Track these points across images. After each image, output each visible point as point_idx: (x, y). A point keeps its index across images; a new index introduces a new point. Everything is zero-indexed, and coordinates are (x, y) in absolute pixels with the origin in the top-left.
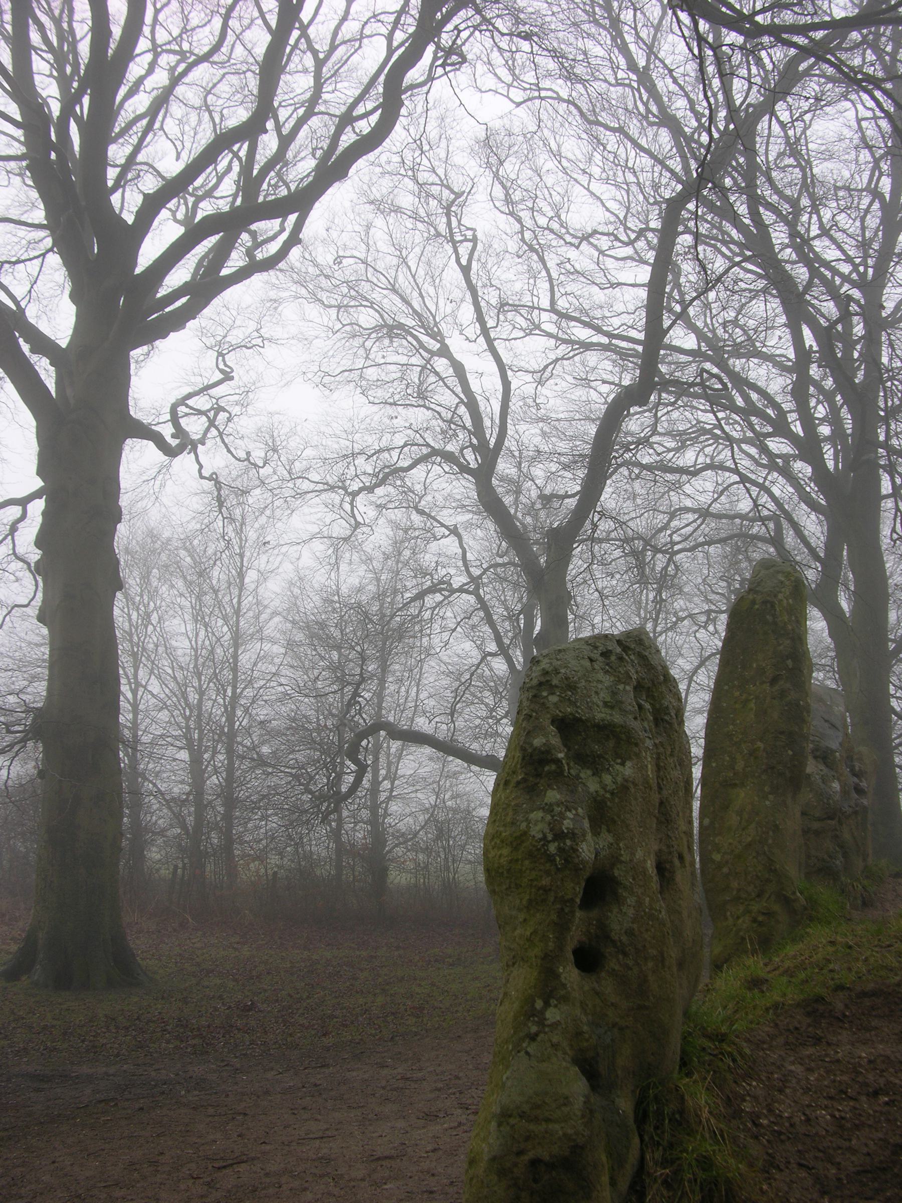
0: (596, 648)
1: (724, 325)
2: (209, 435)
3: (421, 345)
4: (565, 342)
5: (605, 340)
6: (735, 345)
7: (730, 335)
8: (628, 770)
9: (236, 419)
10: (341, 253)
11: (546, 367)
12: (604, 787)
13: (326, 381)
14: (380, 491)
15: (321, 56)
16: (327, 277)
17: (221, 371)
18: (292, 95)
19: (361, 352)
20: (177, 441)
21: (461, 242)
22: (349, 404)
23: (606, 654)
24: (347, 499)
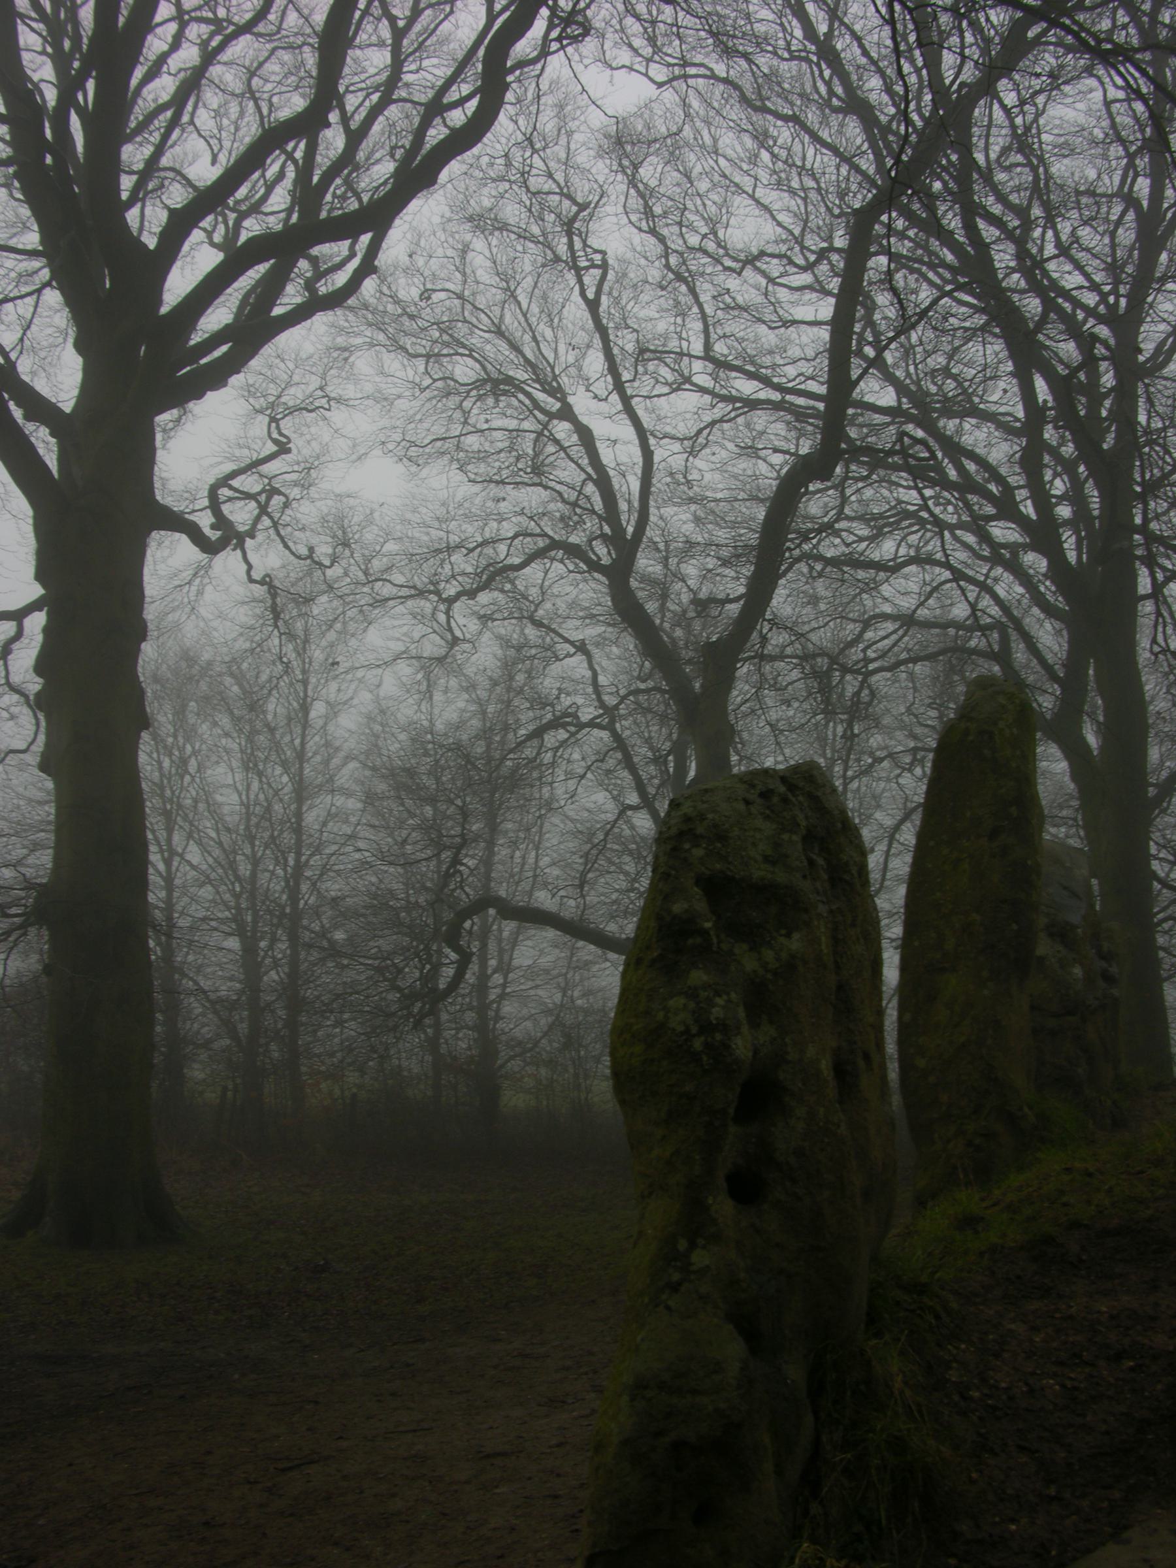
0: (753, 786)
1: (933, 373)
2: (260, 527)
3: (536, 404)
5: (776, 396)
6: (946, 399)
7: (940, 388)
8: (795, 943)
9: (295, 504)
10: (429, 286)
11: (700, 432)
13: (412, 454)
14: (484, 597)
15: (401, 24)
16: (412, 317)
17: (275, 442)
18: (363, 77)
19: (458, 415)
20: (219, 533)
21: (587, 268)
22: (444, 482)
23: (766, 795)
24: (442, 607)
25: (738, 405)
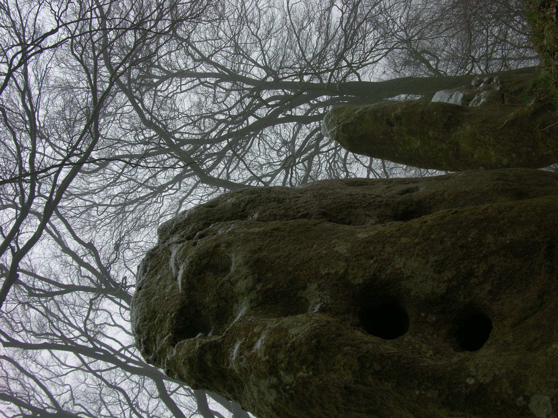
7: (284, 153)
12: (250, 290)
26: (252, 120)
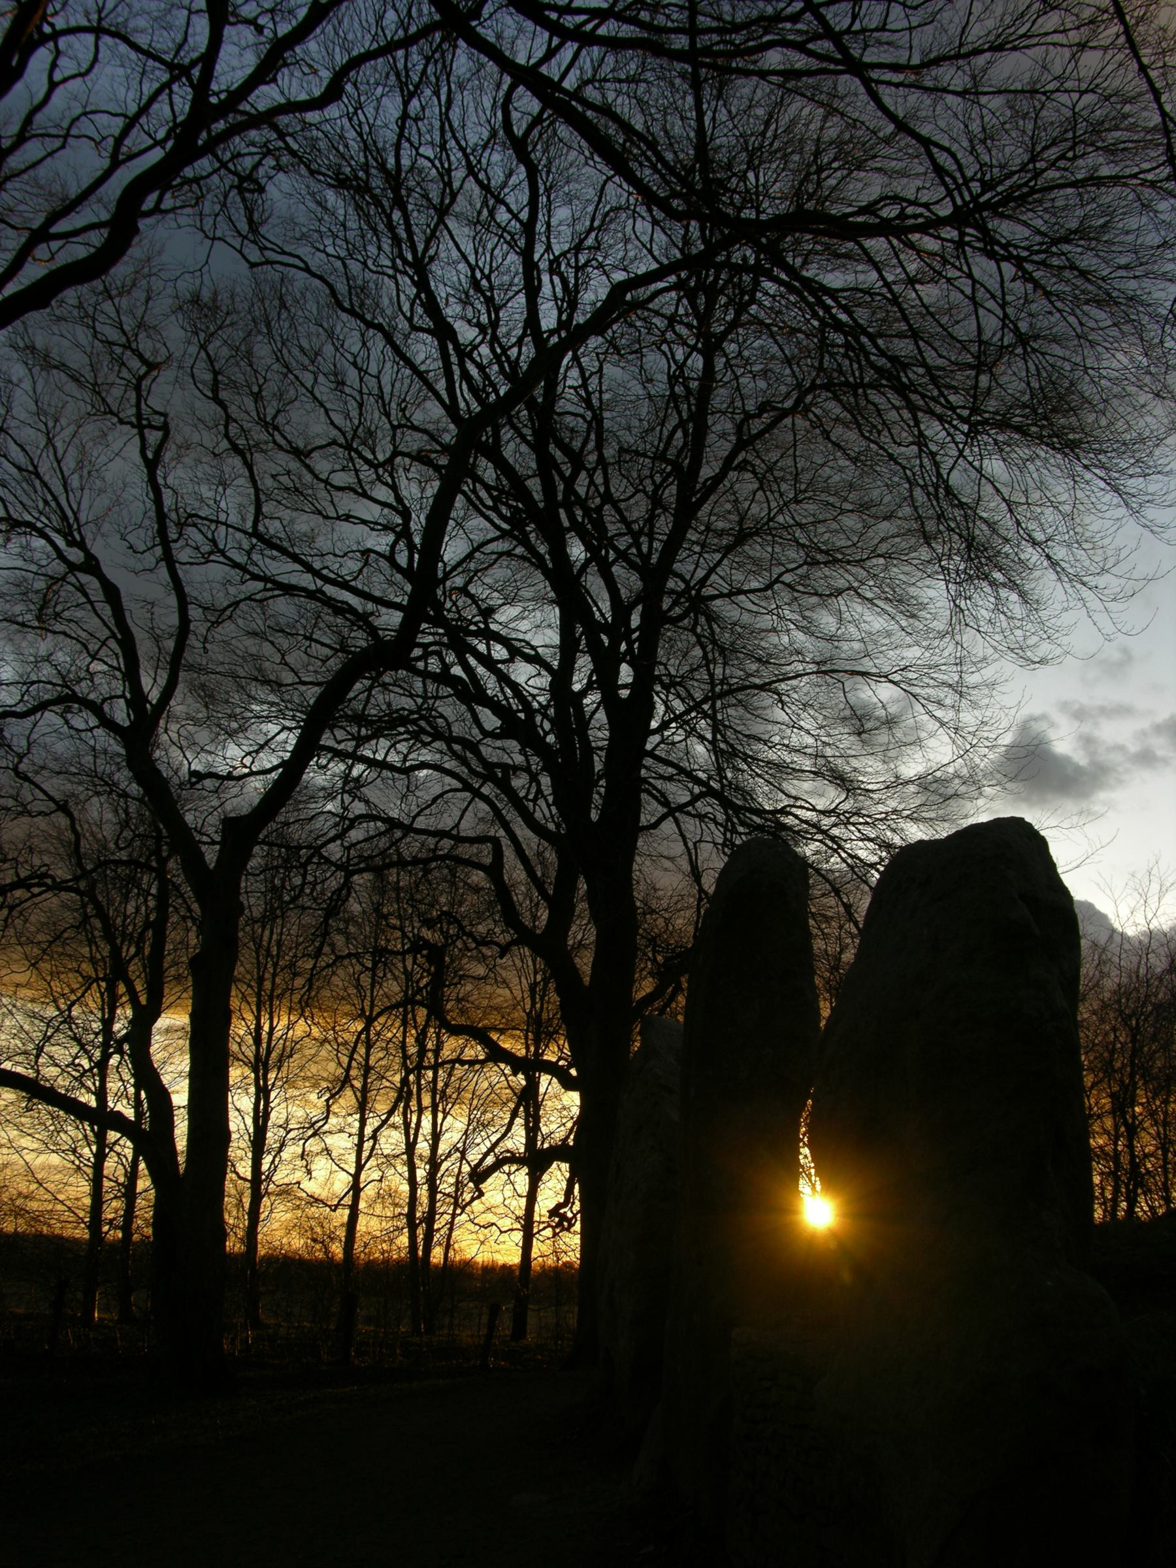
4: (255, 577)
25: (269, 586)
26: (577, 551)
